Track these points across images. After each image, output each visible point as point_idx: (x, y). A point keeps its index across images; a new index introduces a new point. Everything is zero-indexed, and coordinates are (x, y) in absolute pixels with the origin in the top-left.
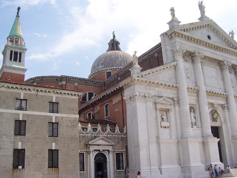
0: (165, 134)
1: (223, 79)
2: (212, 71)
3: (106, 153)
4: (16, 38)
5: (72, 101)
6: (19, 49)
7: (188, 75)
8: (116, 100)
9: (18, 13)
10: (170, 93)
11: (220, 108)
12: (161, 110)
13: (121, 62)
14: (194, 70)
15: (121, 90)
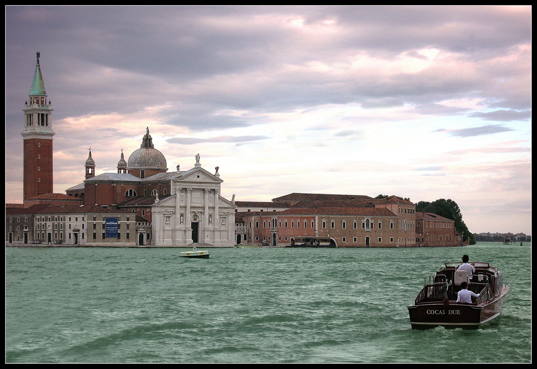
0: (167, 228)
1: (204, 198)
2: (198, 195)
3: (143, 234)
4: (41, 98)
5: (134, 216)
6: (46, 110)
7: (182, 199)
8: (148, 210)
9: (38, 61)
10: (172, 210)
11: (200, 213)
12: (166, 217)
13: (152, 163)
14: (186, 196)
15: (151, 207)
